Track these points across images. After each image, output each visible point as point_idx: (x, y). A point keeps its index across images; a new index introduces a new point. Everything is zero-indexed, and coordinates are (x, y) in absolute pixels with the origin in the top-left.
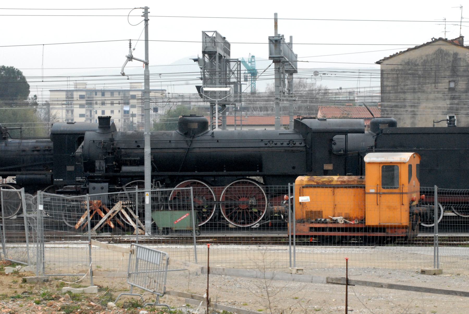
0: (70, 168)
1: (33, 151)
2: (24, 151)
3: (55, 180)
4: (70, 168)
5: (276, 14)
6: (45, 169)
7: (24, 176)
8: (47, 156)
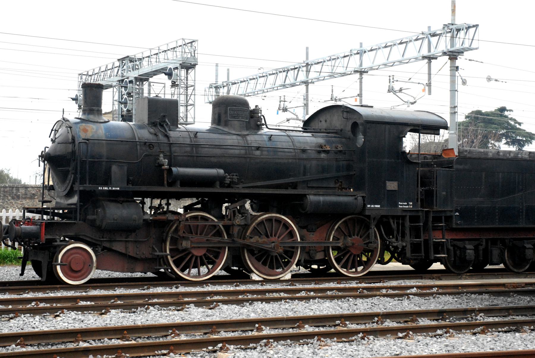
0: (392, 186)
1: (319, 152)
2: (304, 151)
3: (369, 206)
4: (392, 186)
5: (307, 48)
6: (337, 185)
7: (321, 198)
8: (341, 163)
